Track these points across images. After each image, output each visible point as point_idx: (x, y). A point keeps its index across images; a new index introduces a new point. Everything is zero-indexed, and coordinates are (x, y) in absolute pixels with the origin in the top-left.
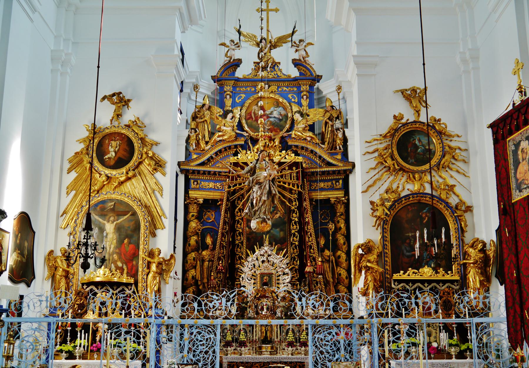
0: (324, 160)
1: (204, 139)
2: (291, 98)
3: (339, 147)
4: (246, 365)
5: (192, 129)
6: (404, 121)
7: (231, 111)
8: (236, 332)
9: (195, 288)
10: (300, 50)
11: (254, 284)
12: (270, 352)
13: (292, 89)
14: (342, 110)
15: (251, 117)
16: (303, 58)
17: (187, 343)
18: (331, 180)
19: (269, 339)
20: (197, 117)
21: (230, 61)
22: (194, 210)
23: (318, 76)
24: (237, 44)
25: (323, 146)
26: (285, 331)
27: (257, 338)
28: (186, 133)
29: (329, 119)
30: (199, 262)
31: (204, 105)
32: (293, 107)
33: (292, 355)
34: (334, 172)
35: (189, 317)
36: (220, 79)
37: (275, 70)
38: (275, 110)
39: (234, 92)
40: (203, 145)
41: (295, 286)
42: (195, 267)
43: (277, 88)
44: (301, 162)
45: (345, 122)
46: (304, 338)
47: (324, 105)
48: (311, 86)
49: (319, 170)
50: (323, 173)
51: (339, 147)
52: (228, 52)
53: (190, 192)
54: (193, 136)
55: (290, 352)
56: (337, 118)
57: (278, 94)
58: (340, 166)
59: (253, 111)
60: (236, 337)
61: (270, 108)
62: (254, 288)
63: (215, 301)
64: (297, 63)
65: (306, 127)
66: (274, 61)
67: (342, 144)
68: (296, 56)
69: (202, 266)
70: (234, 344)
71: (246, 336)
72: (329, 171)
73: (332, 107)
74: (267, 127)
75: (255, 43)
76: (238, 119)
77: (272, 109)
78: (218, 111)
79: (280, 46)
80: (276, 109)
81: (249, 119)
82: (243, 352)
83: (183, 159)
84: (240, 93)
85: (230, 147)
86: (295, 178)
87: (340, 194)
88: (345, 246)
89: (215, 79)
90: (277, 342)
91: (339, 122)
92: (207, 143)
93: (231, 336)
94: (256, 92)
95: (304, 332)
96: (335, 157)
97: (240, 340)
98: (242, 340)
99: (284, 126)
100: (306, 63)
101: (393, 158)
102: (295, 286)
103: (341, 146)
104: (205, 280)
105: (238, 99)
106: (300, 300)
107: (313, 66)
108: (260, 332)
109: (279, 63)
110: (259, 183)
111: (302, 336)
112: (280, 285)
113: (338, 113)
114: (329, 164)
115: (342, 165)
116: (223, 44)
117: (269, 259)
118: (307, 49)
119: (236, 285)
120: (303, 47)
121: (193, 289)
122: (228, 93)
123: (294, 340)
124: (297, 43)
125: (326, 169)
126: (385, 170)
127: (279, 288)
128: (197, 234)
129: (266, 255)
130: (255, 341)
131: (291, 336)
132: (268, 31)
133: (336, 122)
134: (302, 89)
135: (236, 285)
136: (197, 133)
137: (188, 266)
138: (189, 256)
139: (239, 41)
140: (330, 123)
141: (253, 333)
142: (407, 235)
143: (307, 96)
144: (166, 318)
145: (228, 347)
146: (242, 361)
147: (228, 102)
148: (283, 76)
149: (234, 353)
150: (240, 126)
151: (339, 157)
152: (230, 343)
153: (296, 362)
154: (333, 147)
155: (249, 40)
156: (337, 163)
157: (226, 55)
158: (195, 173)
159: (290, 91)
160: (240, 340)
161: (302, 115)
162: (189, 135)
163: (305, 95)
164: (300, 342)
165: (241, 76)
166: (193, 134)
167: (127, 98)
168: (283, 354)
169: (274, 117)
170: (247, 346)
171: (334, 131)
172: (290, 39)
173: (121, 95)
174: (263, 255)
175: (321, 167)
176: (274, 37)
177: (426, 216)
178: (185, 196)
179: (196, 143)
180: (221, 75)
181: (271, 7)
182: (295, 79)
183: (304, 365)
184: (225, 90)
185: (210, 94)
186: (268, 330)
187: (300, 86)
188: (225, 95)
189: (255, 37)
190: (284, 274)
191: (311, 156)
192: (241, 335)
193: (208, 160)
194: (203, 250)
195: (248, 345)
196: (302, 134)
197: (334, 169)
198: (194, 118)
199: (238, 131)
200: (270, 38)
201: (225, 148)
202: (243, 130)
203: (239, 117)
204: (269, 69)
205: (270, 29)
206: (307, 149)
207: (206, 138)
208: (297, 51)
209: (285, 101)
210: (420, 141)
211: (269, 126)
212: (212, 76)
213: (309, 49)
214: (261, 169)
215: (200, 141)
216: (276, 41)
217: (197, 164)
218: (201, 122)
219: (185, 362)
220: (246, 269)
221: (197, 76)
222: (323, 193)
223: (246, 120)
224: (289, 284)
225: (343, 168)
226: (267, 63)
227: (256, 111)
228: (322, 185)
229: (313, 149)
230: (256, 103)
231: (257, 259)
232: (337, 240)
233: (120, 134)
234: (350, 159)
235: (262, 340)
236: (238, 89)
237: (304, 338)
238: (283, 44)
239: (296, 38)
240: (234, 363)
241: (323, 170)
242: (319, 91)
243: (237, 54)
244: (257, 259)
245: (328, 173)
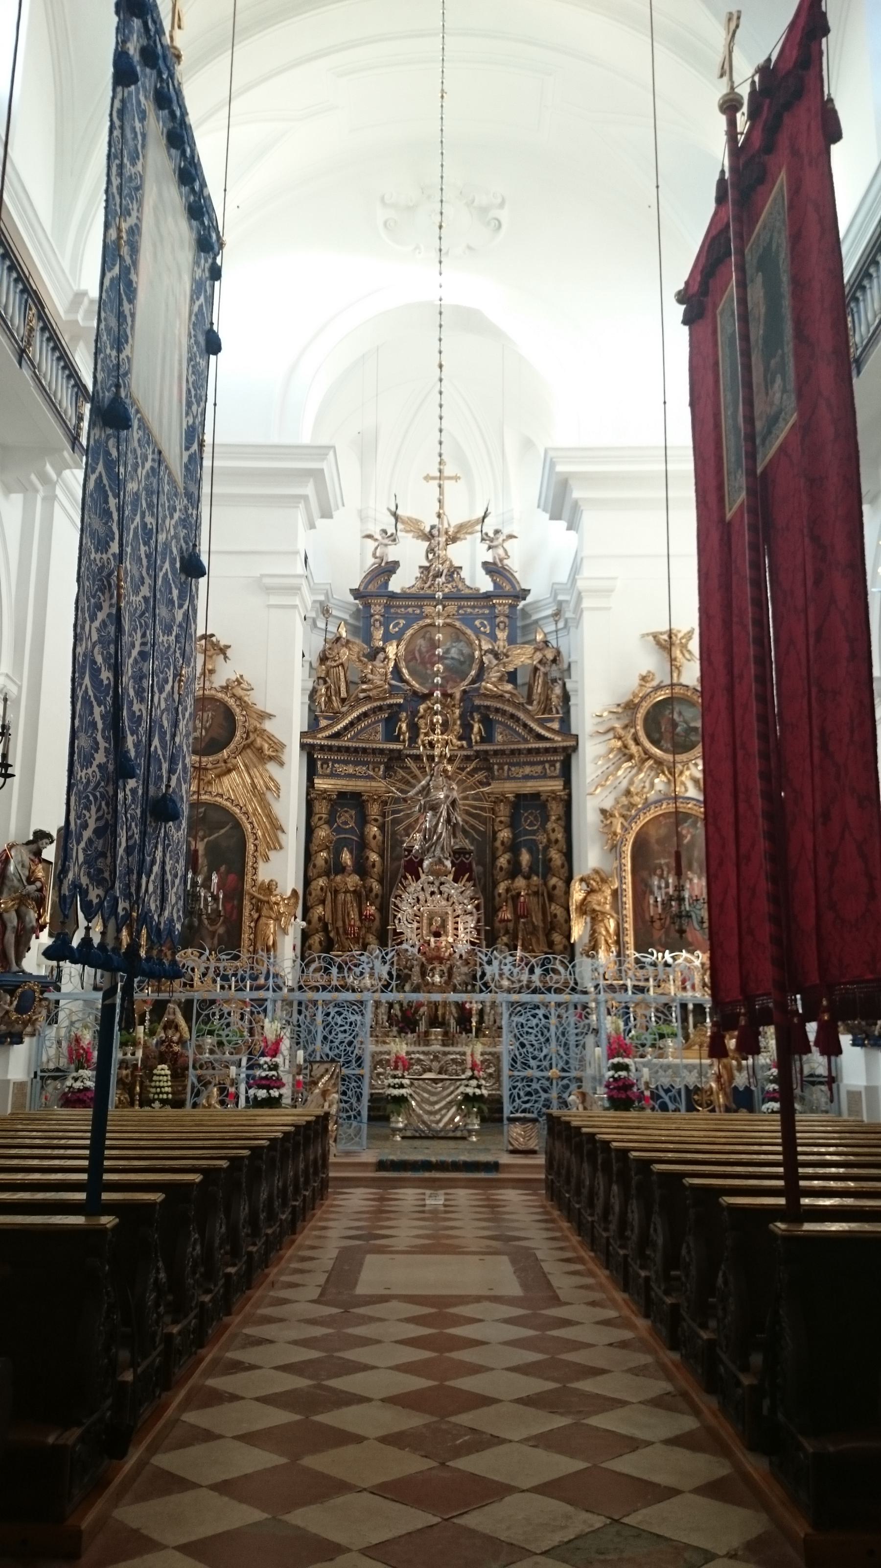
0: (531, 730)
5: (319, 678)
6: (655, 683)
7: (383, 649)
11: (418, 929)
14: (562, 649)
15: (414, 658)
17: (320, 1028)
18: (542, 763)
20: (327, 659)
22: (322, 808)
23: (524, 590)
24: (392, 535)
25: (530, 707)
28: (310, 685)
29: (540, 662)
30: (329, 894)
31: (338, 639)
32: (483, 643)
34: (547, 750)
35: (324, 988)
37: (453, 580)
40: (336, 704)
42: (323, 902)
45: (565, 666)
47: (531, 637)
48: (513, 607)
49: (522, 746)
50: (530, 751)
53: (316, 781)
58: (557, 741)
63: (364, 965)
64: (491, 569)
65: (503, 676)
66: (451, 565)
68: (489, 557)
69: (334, 901)
78: (359, 646)
83: (306, 729)
84: (396, 618)
85: (380, 709)
87: (557, 785)
88: (563, 871)
89: (357, 594)
92: (343, 700)
94: (422, 617)
96: (549, 725)
101: (637, 742)
104: (340, 924)
105: (394, 627)
106: (489, 963)
110: (434, 808)
113: (555, 652)
114: (540, 737)
115: (559, 739)
116: (369, 536)
117: (442, 888)
118: (506, 545)
120: (500, 540)
122: (377, 617)
124: (491, 534)
125: (534, 746)
126: (623, 759)
128: (327, 847)
129: (437, 883)
137: (311, 900)
138: (314, 885)
140: (542, 669)
142: (658, 861)
144: (285, 990)
147: (378, 634)
150: (397, 670)
151: (556, 726)
154: (547, 709)
161: (496, 655)
162: (314, 688)
165: (398, 590)
167: (222, 643)
169: (453, 658)
172: (478, 528)
173: (214, 639)
174: (433, 883)
175: (526, 741)
176: (453, 524)
177: (688, 832)
178: (308, 787)
180: (366, 587)
181: (447, 484)
182: (487, 596)
185: (347, 617)
190: (466, 913)
191: (510, 723)
193: (346, 728)
194: (336, 874)
197: (548, 745)
198: (323, 659)
199: (393, 682)
202: (402, 680)
208: (490, 548)
209: (469, 631)
210: (680, 714)
212: (351, 590)
213: (508, 545)
214: (437, 788)
219: (318, 1059)
220: (405, 907)
222: (530, 784)
223: (407, 662)
225: (561, 744)
228: (527, 770)
231: (423, 889)
232: (550, 860)
233: (213, 699)
234: (574, 732)
236: (392, 610)
238: (468, 537)
239: (489, 527)
241: (530, 746)
242: (525, 613)
243: (392, 553)
244: (423, 889)
245: (538, 751)
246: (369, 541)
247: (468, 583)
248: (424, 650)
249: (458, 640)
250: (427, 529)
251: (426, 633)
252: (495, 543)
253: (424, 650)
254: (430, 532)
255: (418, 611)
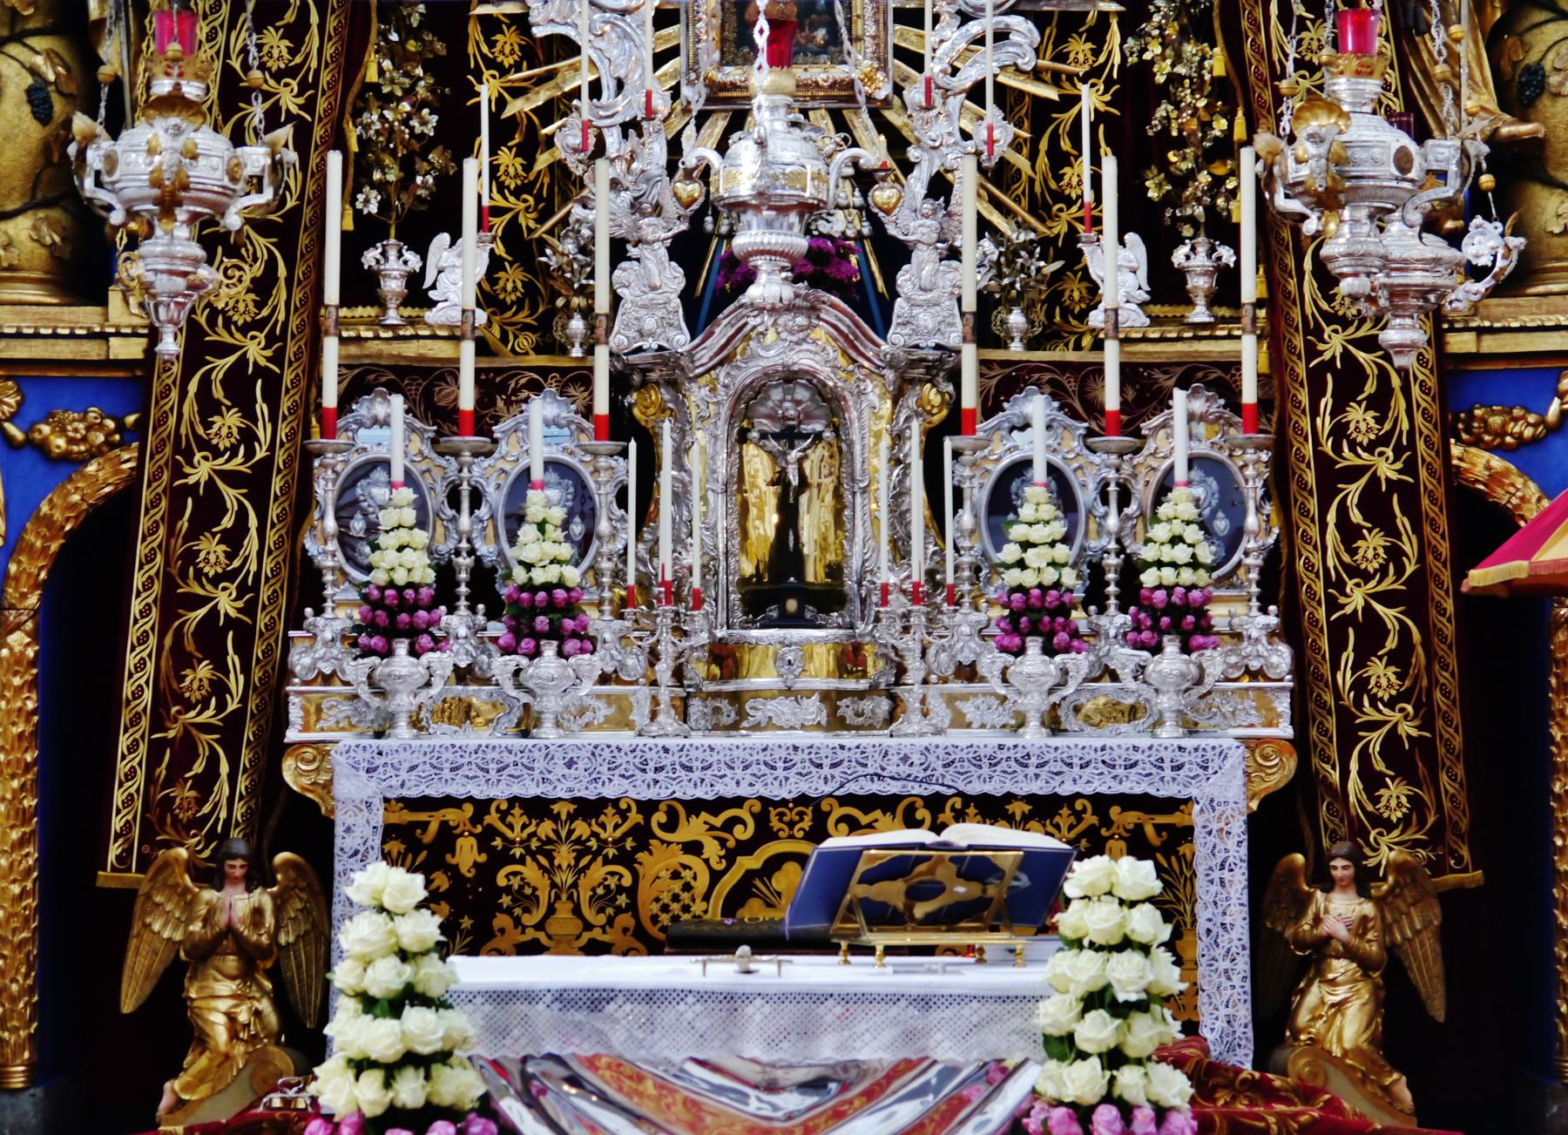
4: (581, 829)
8: (477, 498)
9: (50, 55)
12: (830, 698)
19: (814, 573)
26: (978, 493)
27: (693, 558)
33: (1054, 725)
41: (1079, 48)
46: (1181, 554)
55: (1034, 703)
60: (485, 549)
62: (660, 59)
70: (457, 622)
71: (584, 545)
82: (549, 704)
90: (898, 603)
93: (421, 537)
95: (1178, 493)
97: (520, 575)
98: (539, 576)
102: (1079, 48)
108: (719, 503)
111: (1160, 532)
112: (930, 35)
119: (474, 31)
121: (33, 71)
123: (1069, 578)
127: (915, 60)
130: (675, 593)
131: (1038, 534)
135: (474, 31)
141: (646, 515)
145: (388, 653)
146: (530, 790)
149: (465, 714)
152: (413, 608)
153: (1101, 802)
160: (520, 575)
164: (1131, 594)
168: (960, 722)
170: (589, 643)
183: (1187, 833)
186: (804, 484)
192: (527, 532)
195: (600, 623)
224: (1016, 21)
235: (744, 581)
237: (1181, 554)
240: (451, 815)
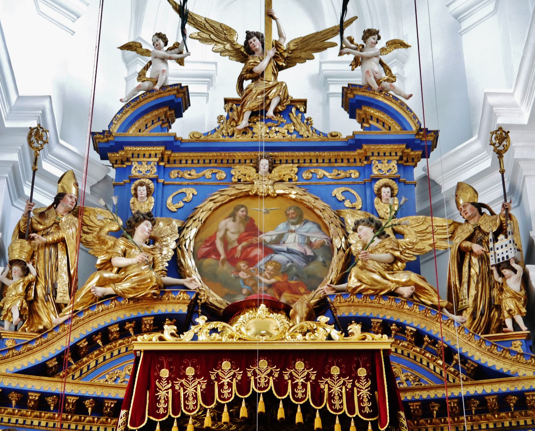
1: (51, 298)
2: (340, 197)
3: (514, 321)
5: (12, 263)
10: (369, 58)
13: (343, 174)
15: (214, 251)
16: (379, 82)
21: (150, 91)
24: (176, 46)
29: (470, 239)
36: (117, 140)
38: (292, 232)
39: (161, 181)
43: (296, 170)
44: (387, 352)
51: (514, 321)
52: (146, 68)
54: (16, 286)
56: (501, 230)
57: (300, 186)
59: (220, 235)
61: (274, 228)
65: (396, 259)
67: (524, 310)
72: (482, 398)
73: (480, 206)
74: (264, 280)
75: (228, 46)
76: (171, 253)
77: (282, 227)
79: (303, 60)
80: (293, 228)
81: (206, 255)
84: (181, 185)
86: (367, 405)
91: (506, 241)
99: (319, 275)
100: (387, 96)
103: (520, 320)
107: (408, 102)
109: (304, 102)
124: (359, 41)
132: (270, 16)
133: (497, 245)
134: (375, 172)
136: (30, 277)
139: (180, 40)
140: (476, 248)
143: (392, 190)
148: (316, 136)
155: (212, 36)
156: (513, 369)
157: (141, 76)
158: (10, 405)
159: (337, 178)
163: (386, 185)
166: (16, 278)
169: (289, 251)
171: (491, 272)
179: (21, 309)
184: (134, 172)
187: (370, 166)
188: (133, 187)
189: (230, 31)
196: (385, 278)
197: (504, 387)
200: (275, 36)
201: (122, 324)
203: (173, 245)
204: (270, 113)
205: (276, 10)
206: (402, 327)
207: (59, 295)
208: (357, 62)
211: (272, 276)
215: (40, 304)
216: (292, 47)
217: (19, 368)
218: (47, 245)
221: (44, 115)
226: (267, 98)
227: (228, 233)
229: (422, 326)
230: (231, 211)
236: (174, 174)
238: (316, 55)
241: (463, 391)
246: (130, 54)
247: (317, 125)
248: (233, 237)
249: (300, 220)
250: (241, 40)
251: (237, 209)
252: (367, 53)
253: (233, 237)
254: (246, 43)
255: (222, 175)
